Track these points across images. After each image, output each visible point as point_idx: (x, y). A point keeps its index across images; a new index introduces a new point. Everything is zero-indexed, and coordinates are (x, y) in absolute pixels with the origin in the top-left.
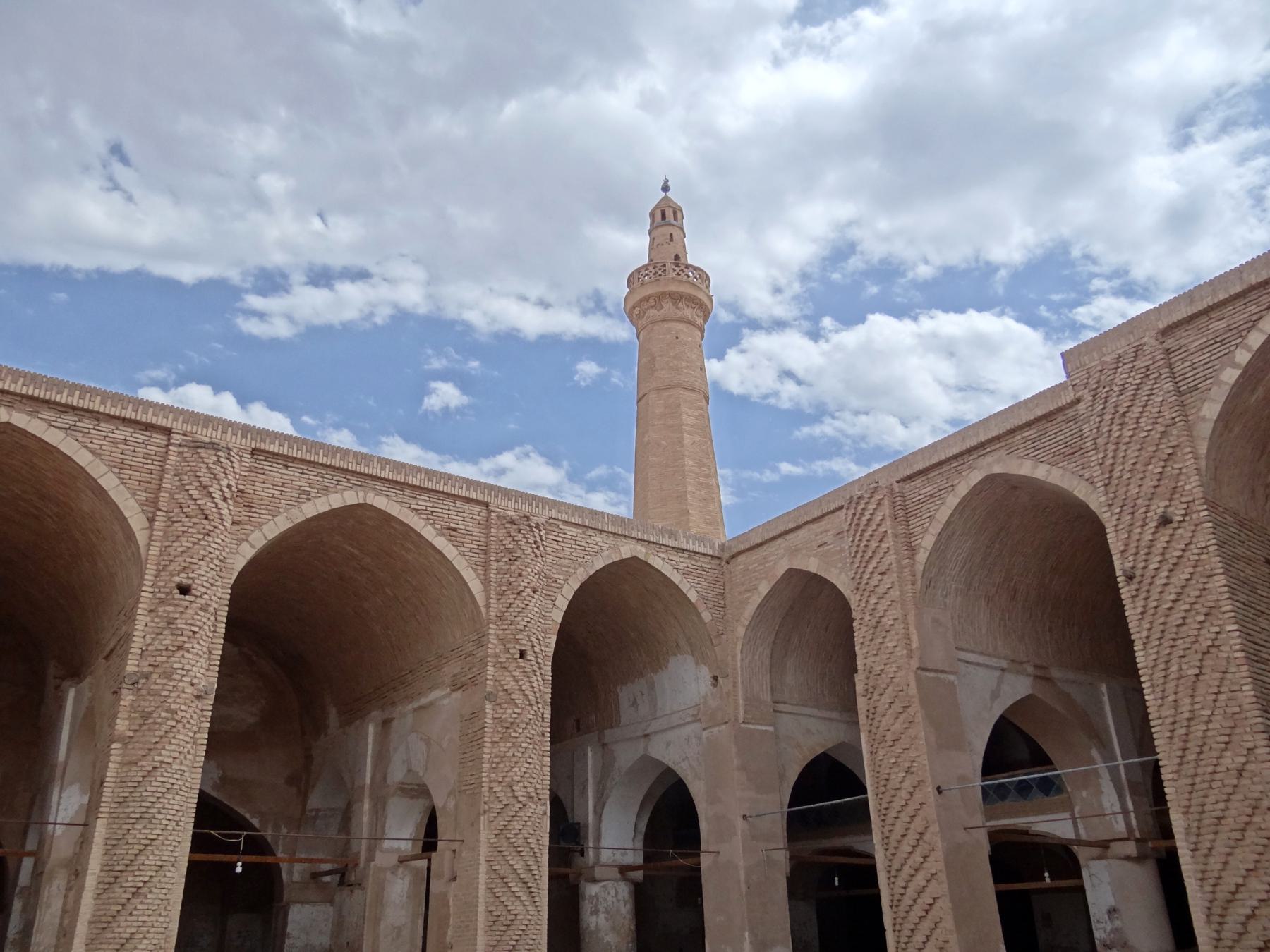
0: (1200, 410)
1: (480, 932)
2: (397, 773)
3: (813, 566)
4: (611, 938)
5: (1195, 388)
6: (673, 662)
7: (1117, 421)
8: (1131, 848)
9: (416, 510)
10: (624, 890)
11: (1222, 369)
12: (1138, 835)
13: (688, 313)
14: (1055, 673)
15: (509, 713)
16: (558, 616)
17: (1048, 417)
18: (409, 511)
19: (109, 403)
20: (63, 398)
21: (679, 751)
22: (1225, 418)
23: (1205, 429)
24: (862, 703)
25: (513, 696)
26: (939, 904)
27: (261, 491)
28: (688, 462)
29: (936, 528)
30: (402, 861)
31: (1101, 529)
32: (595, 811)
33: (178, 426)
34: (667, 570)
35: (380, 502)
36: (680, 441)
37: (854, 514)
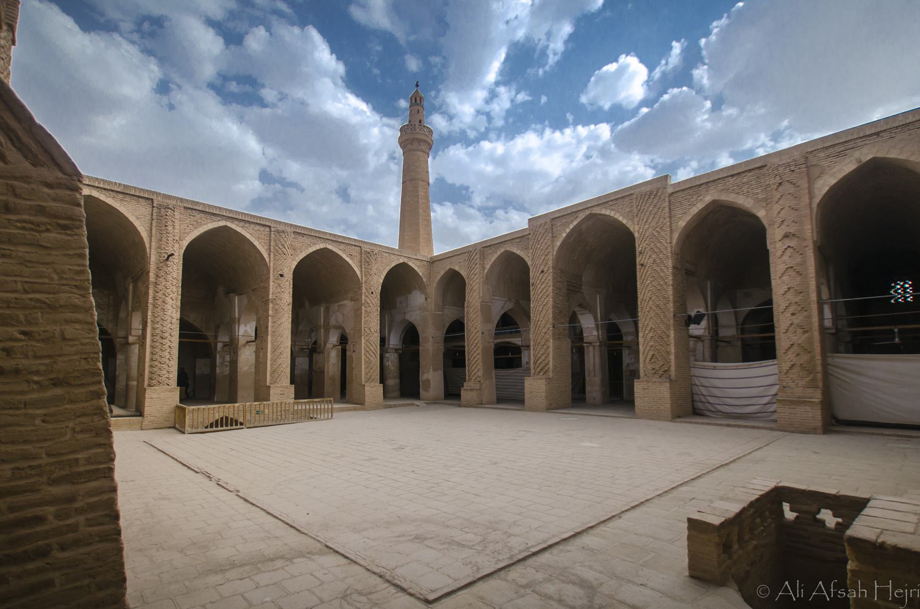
2: (333, 322)
3: (457, 269)
4: (392, 368)
6: (414, 292)
10: (396, 355)
13: (423, 147)
14: (521, 302)
15: (368, 309)
16: (381, 281)
17: (522, 237)
20: (240, 217)
21: (414, 317)
22: (562, 246)
27: (297, 245)
28: (420, 211)
29: (490, 263)
33: (272, 225)
34: (413, 266)
35: (330, 247)
36: (418, 202)
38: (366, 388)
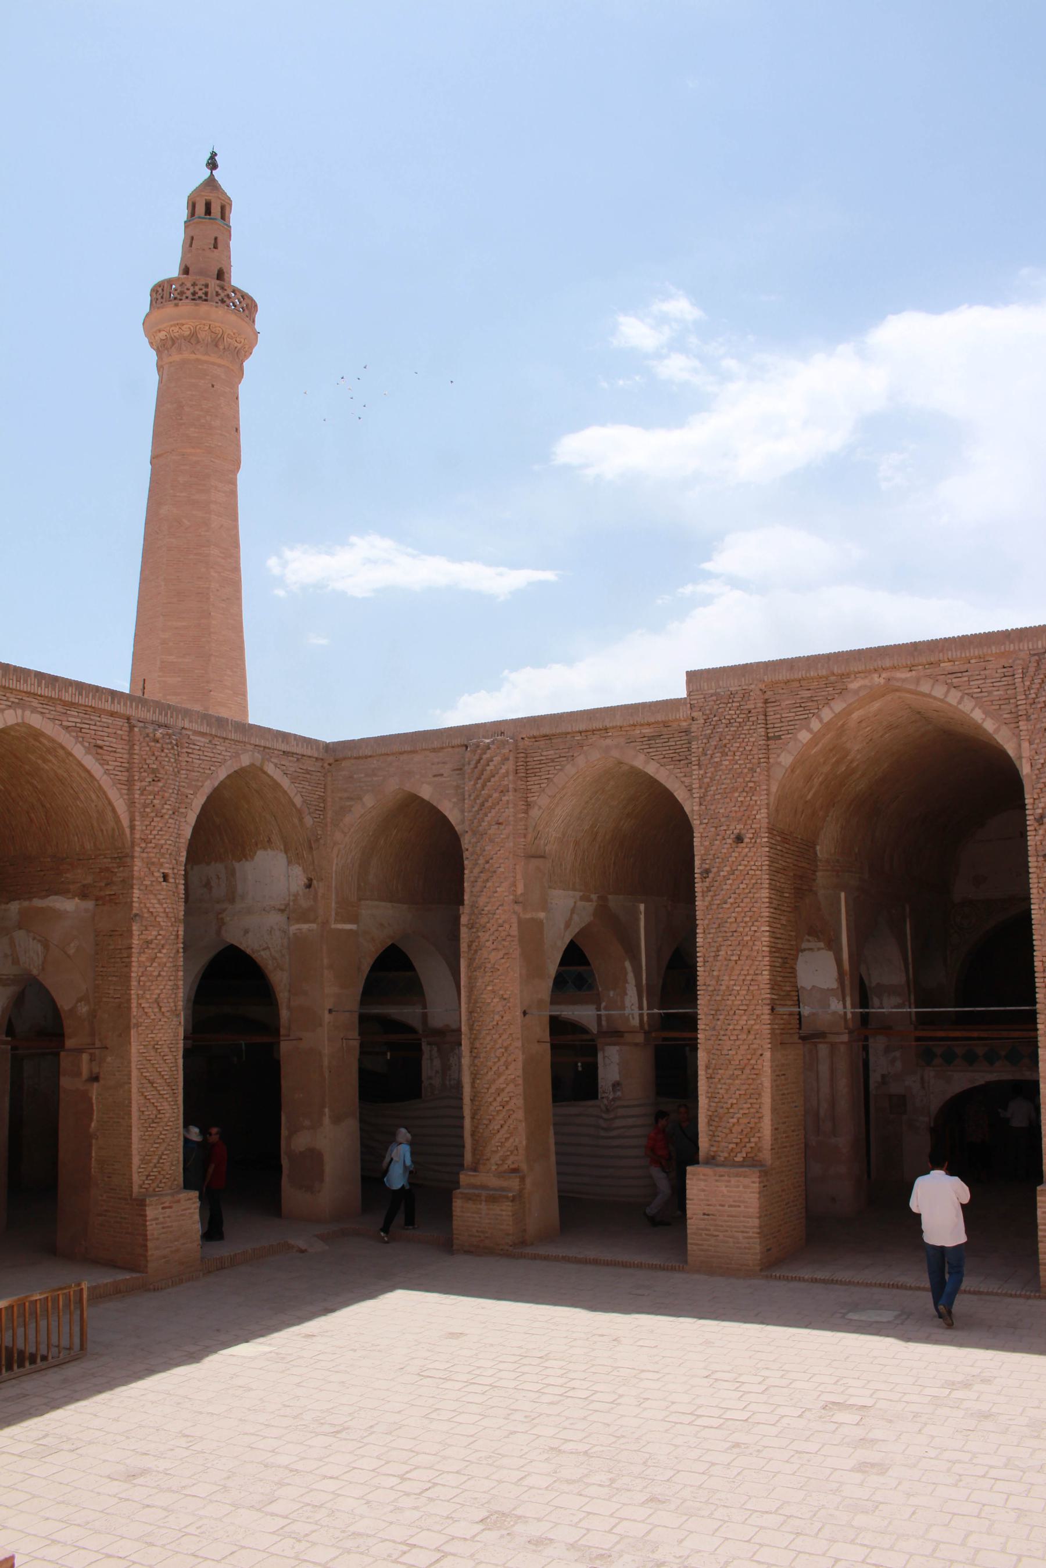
0: (779, 756)
1: (134, 1129)
3: (426, 792)
5: (779, 738)
6: (260, 854)
8: (640, 1038)
11: (800, 730)
12: (646, 1027)
16: (188, 832)
18: (60, 728)
23: (778, 773)
24: (464, 932)
25: (159, 919)
26: (514, 1101)
35: (35, 720)
37: (479, 761)
38: (151, 1212)
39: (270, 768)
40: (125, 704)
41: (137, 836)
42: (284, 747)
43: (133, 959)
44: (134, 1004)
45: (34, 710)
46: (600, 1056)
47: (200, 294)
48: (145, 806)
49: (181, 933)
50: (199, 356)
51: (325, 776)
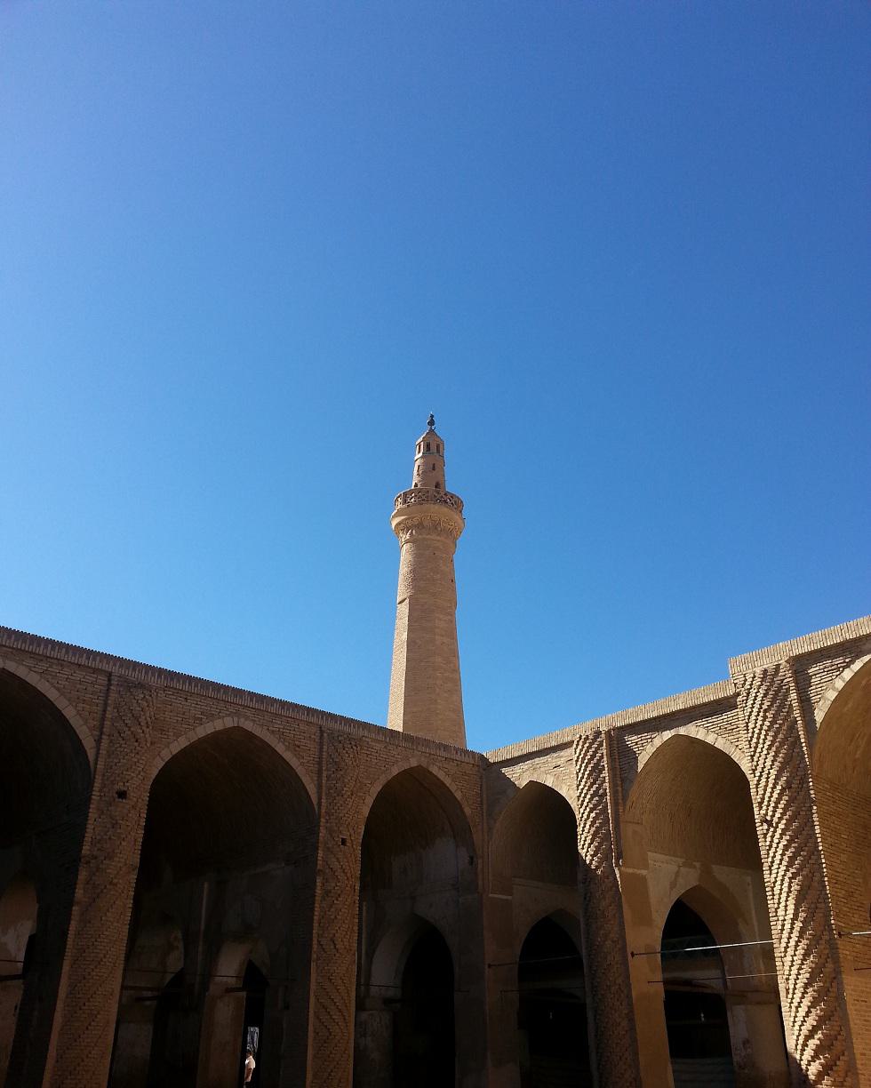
7: (761, 714)
9: (273, 731)
19: (70, 654)
30: (229, 990)
31: (747, 783)
32: (367, 954)
37: (581, 750)
39: (434, 770)
40: (318, 717)
41: (323, 811)
42: (444, 754)
43: (316, 905)
44: (315, 942)
45: (247, 718)
46: (729, 1014)
47: (424, 497)
48: (330, 788)
49: (357, 888)
50: (424, 536)
51: (481, 778)
